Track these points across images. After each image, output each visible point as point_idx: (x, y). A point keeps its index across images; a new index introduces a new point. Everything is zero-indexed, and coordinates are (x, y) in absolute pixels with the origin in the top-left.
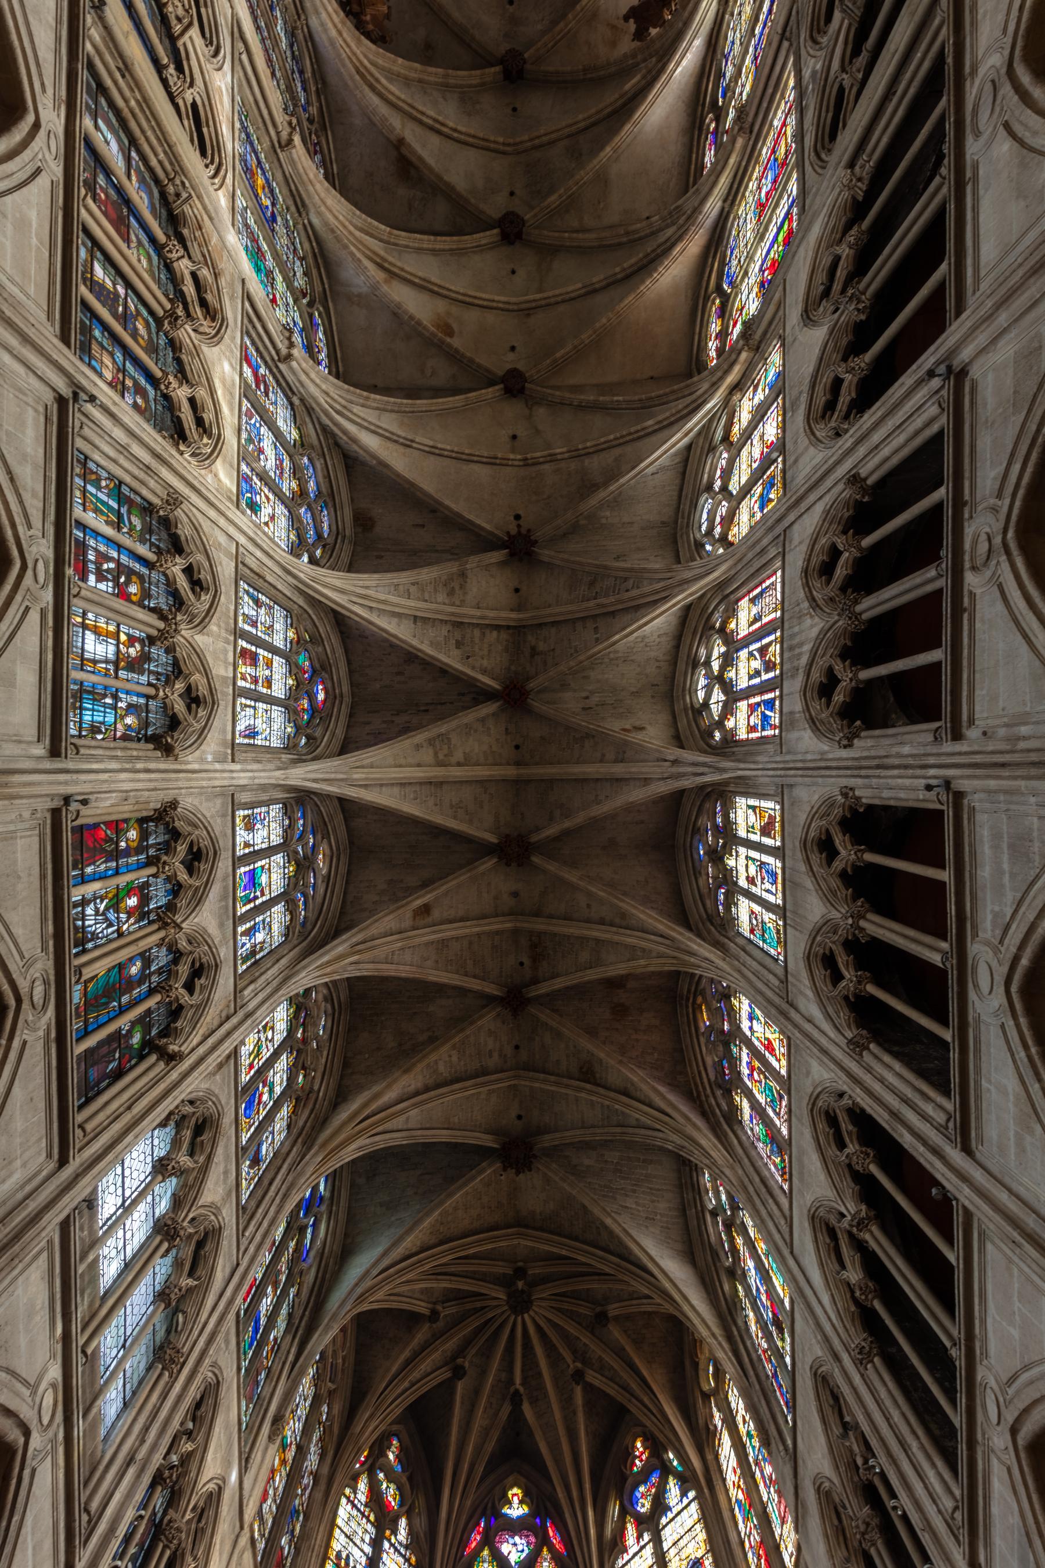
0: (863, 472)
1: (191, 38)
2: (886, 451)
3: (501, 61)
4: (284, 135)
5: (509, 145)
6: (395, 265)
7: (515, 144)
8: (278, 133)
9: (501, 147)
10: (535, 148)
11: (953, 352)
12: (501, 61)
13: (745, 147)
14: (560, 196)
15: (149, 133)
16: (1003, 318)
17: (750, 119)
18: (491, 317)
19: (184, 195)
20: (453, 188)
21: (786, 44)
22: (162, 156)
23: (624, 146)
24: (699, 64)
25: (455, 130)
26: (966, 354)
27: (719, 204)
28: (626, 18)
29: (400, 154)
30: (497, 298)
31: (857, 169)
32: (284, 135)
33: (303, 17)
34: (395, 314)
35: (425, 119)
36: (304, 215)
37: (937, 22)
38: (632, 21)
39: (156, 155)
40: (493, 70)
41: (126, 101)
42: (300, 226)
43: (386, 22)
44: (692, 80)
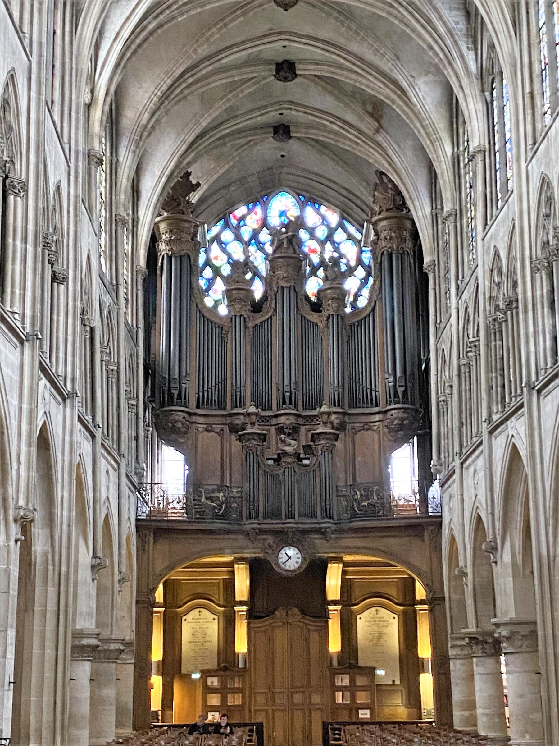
0: (62, 287)
1: (474, 337)
2: (62, 318)
3: (291, 137)
4: (452, 219)
5: (287, 109)
6: (391, 90)
7: (282, 108)
8: (456, 222)
9: (293, 107)
10: (266, 107)
11: (72, 407)
12: (291, 137)
13: (117, 208)
14: (242, 91)
15: (493, 357)
16: (67, 438)
17: (119, 228)
18: (308, 30)
19: (491, 319)
20: (337, 98)
21: (114, 282)
22: (493, 343)
23: (191, 125)
24: (142, 178)
25: (331, 122)
26: (68, 410)
27: (121, 159)
28: (198, 185)
29: (378, 121)
30: (302, 46)
31: (88, 329)
32: (452, 219)
33: (434, 214)
34: (398, 58)
35: (356, 133)
36: (456, 155)
37: (89, 411)
38: (194, 182)
39: (495, 345)
40: (298, 135)
41: (496, 377)
42: (461, 148)
43: (378, 182)
44: (144, 166)
